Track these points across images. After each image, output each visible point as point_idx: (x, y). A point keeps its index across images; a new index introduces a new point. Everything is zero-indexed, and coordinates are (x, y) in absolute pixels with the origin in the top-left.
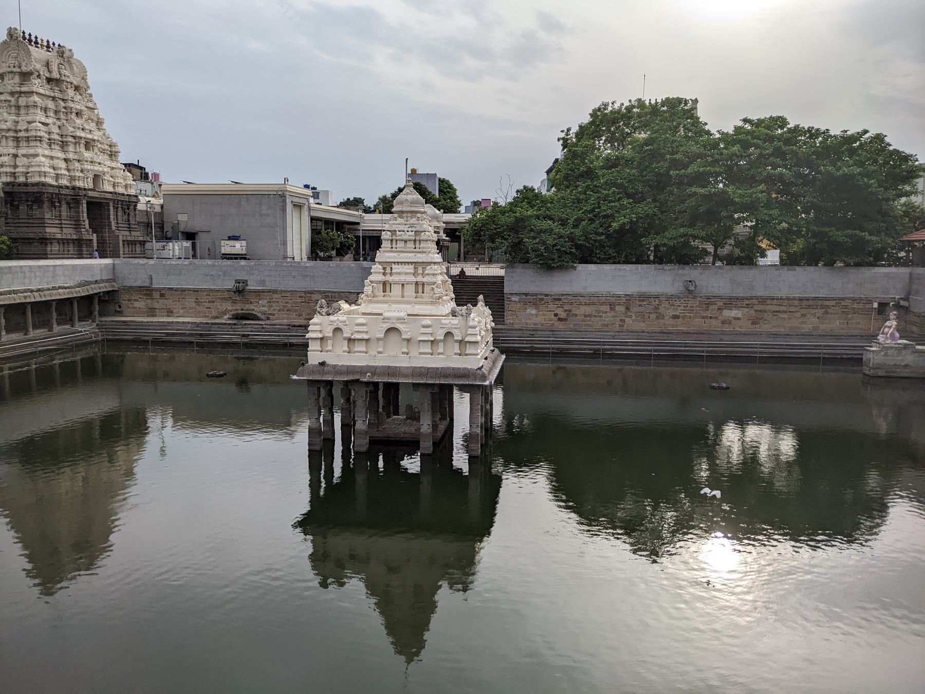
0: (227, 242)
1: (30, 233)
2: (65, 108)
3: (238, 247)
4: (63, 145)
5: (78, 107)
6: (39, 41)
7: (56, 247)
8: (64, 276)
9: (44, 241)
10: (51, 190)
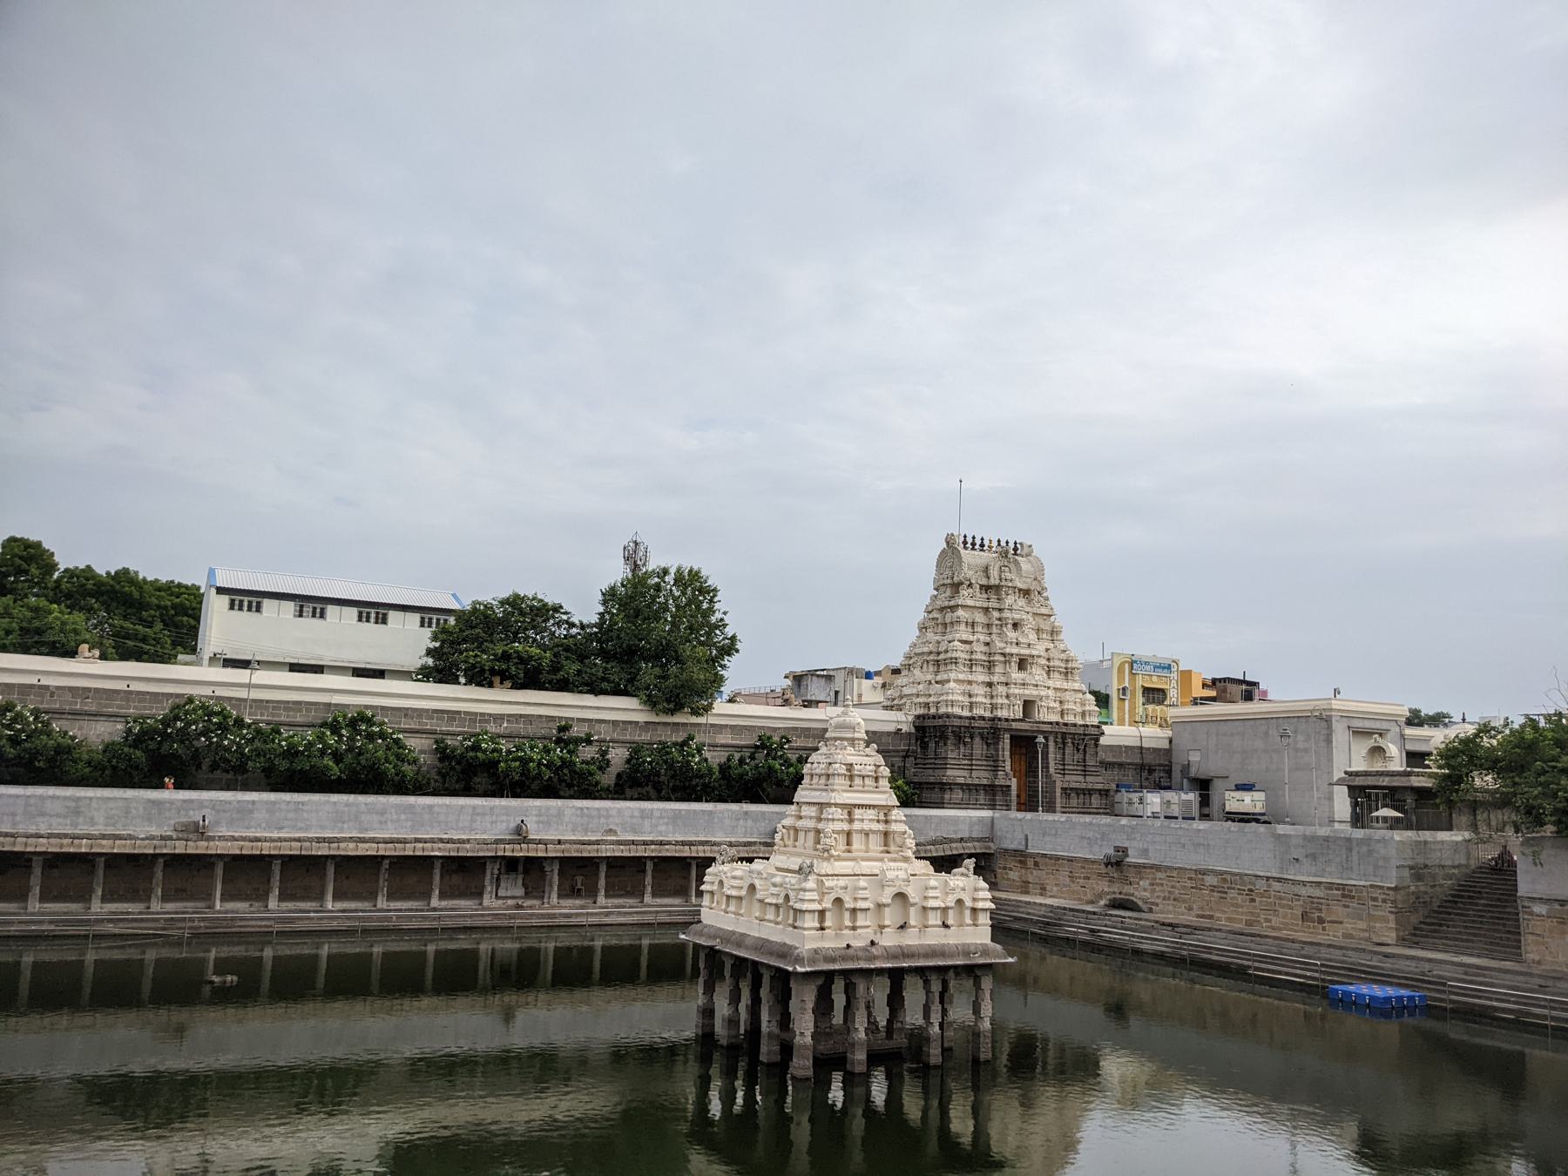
0: (1233, 794)
1: (930, 776)
3: (1250, 802)
4: (990, 666)
5: (1017, 616)
6: (986, 543)
7: (958, 795)
9: (944, 787)
10: (957, 722)
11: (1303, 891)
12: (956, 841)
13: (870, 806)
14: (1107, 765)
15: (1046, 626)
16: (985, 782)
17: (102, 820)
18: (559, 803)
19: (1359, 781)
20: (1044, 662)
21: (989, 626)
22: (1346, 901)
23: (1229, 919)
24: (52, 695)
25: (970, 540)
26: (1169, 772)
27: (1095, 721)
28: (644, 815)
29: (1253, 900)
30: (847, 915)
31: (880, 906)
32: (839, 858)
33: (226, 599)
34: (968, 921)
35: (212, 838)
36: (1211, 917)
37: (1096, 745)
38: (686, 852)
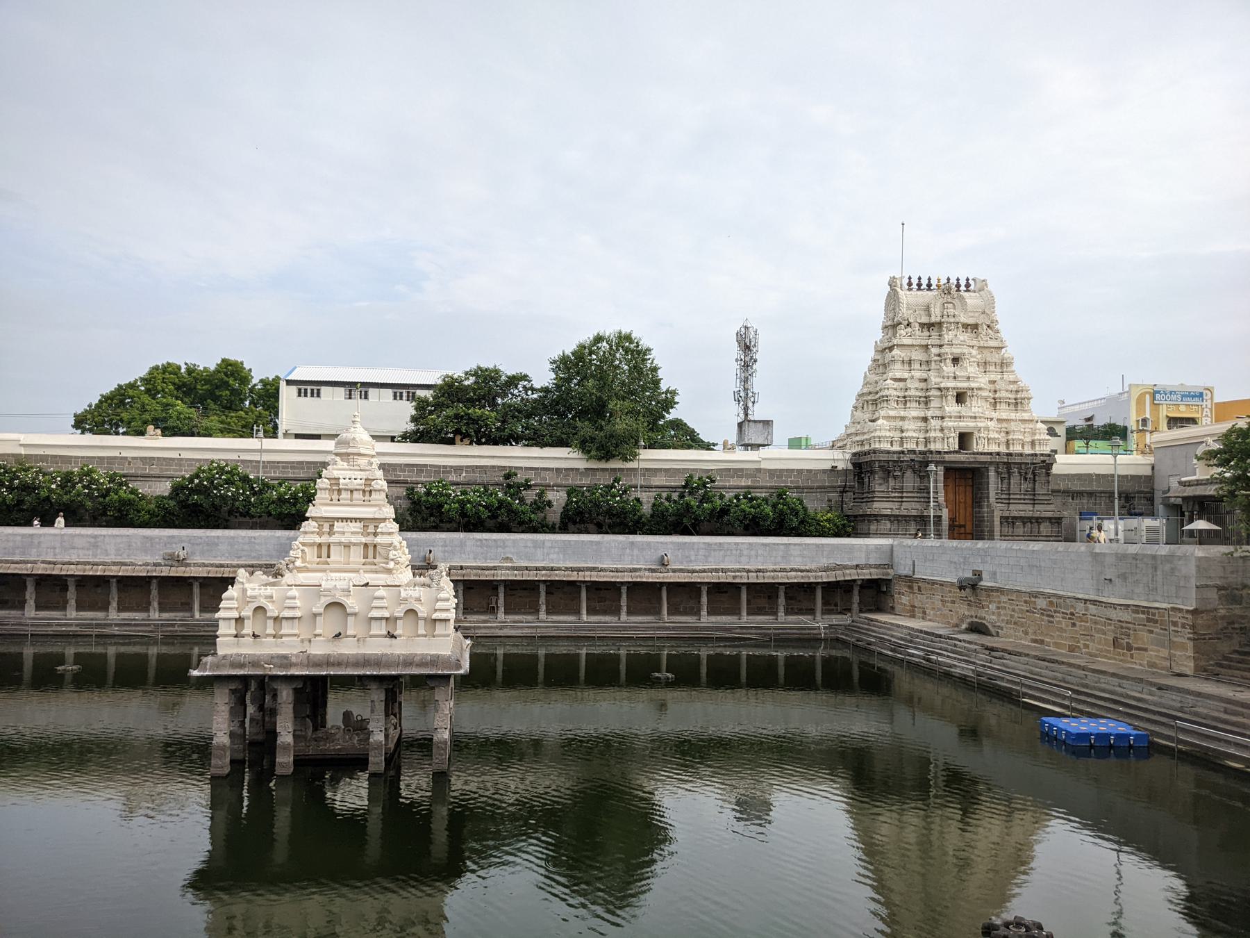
5: (956, 351)
6: (934, 283)
8: (802, 556)
9: (877, 518)
10: (883, 457)
11: (1115, 615)
12: (851, 568)
13: (351, 519)
14: (1075, 494)
15: (994, 357)
16: (914, 513)
17: (113, 552)
19: (1190, 492)
20: (985, 394)
22: (1151, 626)
23: (1057, 645)
24: (129, 463)
25: (915, 281)
26: (1151, 500)
27: (1046, 450)
28: (536, 545)
29: (1074, 625)
30: (270, 623)
31: (315, 615)
32: (307, 570)
33: (294, 389)
34: (421, 631)
35: (188, 565)
36: (1042, 642)
37: (1048, 474)
38: (574, 577)
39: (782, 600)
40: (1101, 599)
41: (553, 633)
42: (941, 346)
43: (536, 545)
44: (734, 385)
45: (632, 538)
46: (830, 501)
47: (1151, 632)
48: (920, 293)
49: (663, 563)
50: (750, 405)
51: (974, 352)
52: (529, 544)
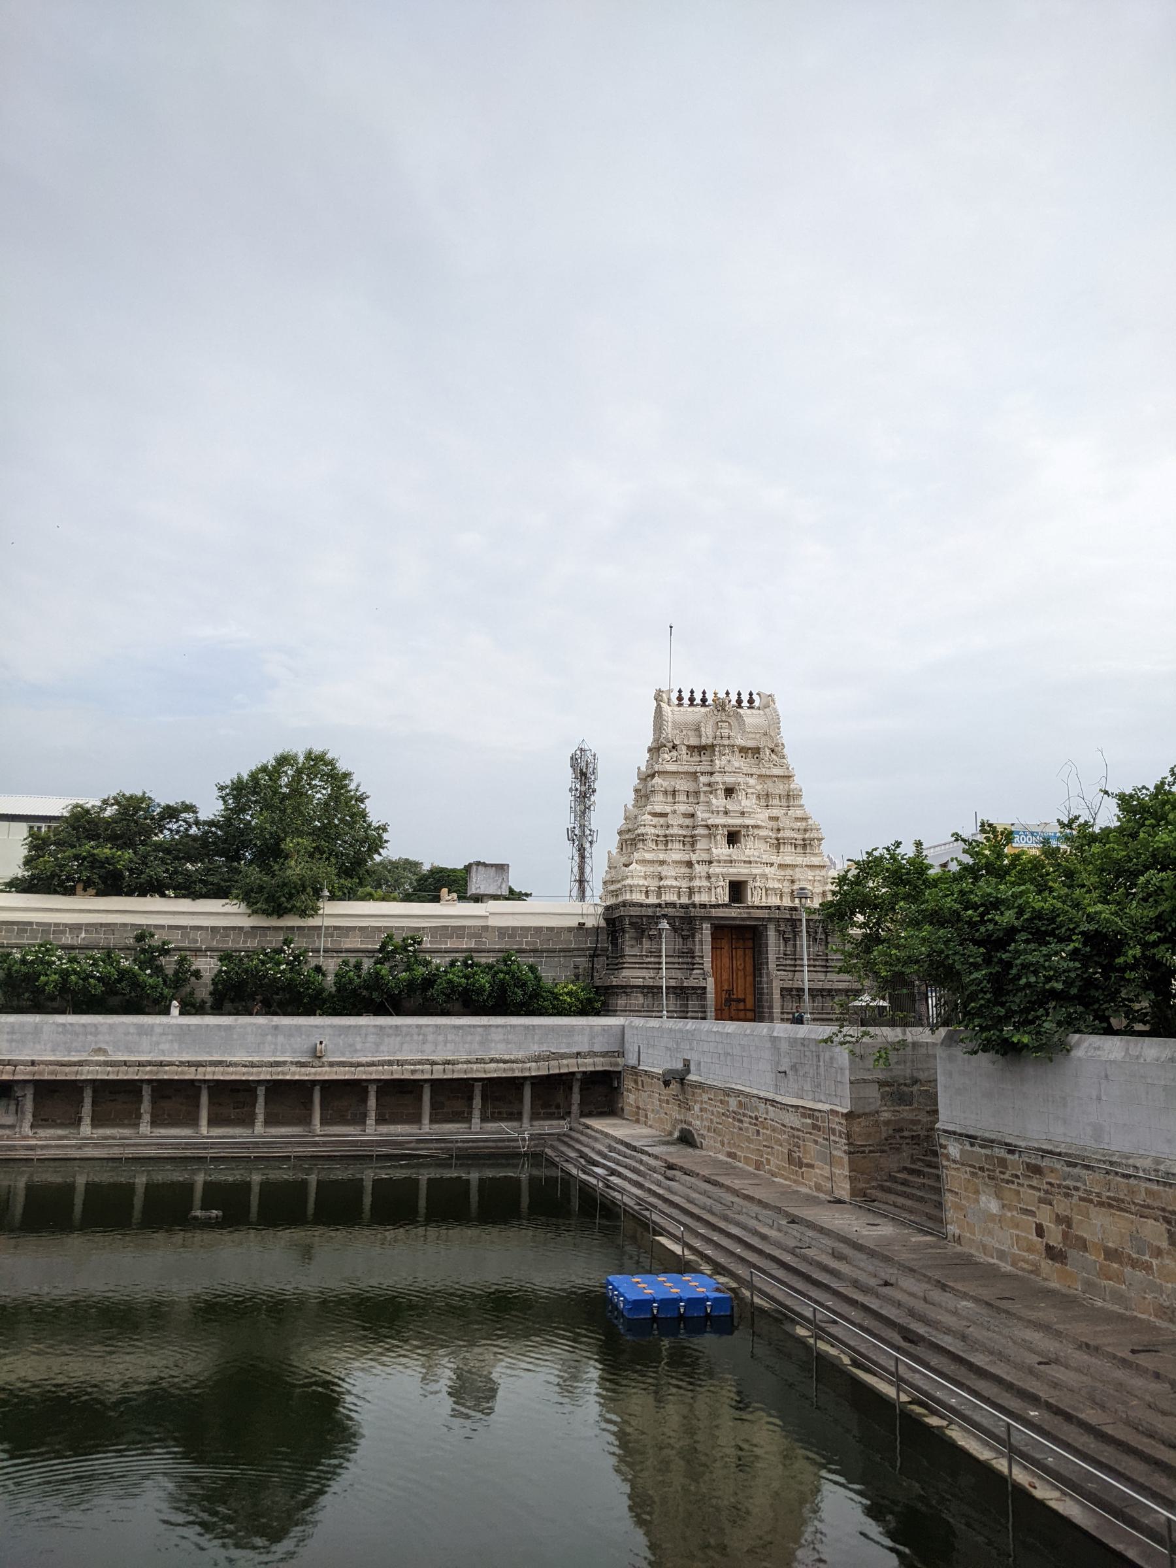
2: (709, 785)
5: (730, 780)
7: (638, 1000)
9: (626, 990)
10: (635, 911)
12: (570, 1056)
15: (780, 788)
18: (37, 1018)
20: (763, 833)
21: (697, 793)
25: (686, 695)
28: (142, 1031)
38: (190, 1074)
39: (477, 1102)
40: (779, 1099)
41: (153, 1152)
42: (712, 774)
43: (142, 1031)
44: (567, 820)
45: (276, 1020)
46: (576, 967)
47: (816, 1142)
48: (691, 709)
49: (317, 1055)
50: (587, 845)
51: (752, 781)
52: (132, 1030)
